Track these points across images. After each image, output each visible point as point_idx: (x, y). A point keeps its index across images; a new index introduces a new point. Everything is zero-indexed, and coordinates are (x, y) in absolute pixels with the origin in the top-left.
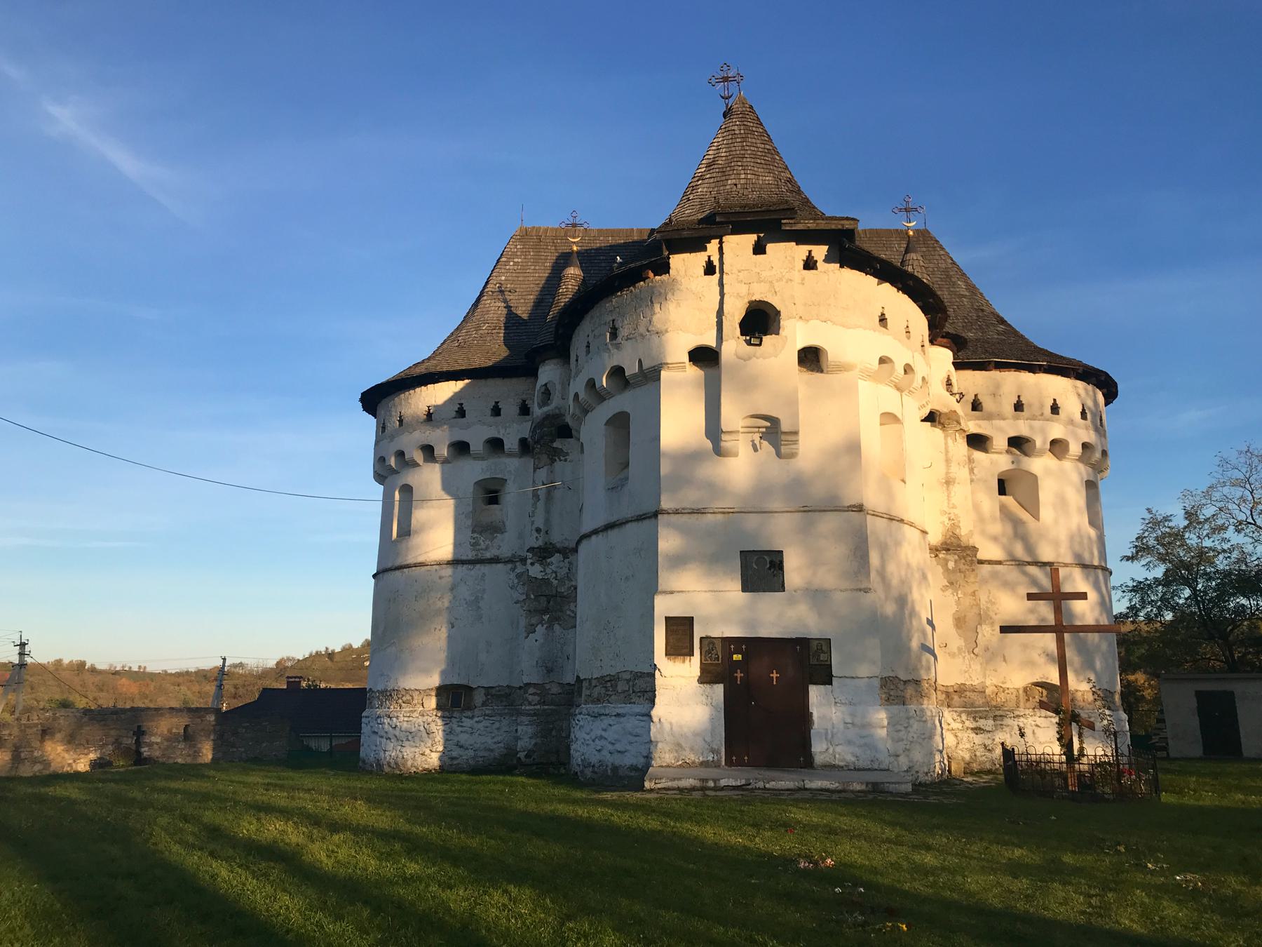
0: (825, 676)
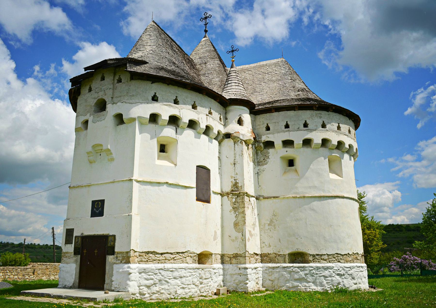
0: (112, 252)
